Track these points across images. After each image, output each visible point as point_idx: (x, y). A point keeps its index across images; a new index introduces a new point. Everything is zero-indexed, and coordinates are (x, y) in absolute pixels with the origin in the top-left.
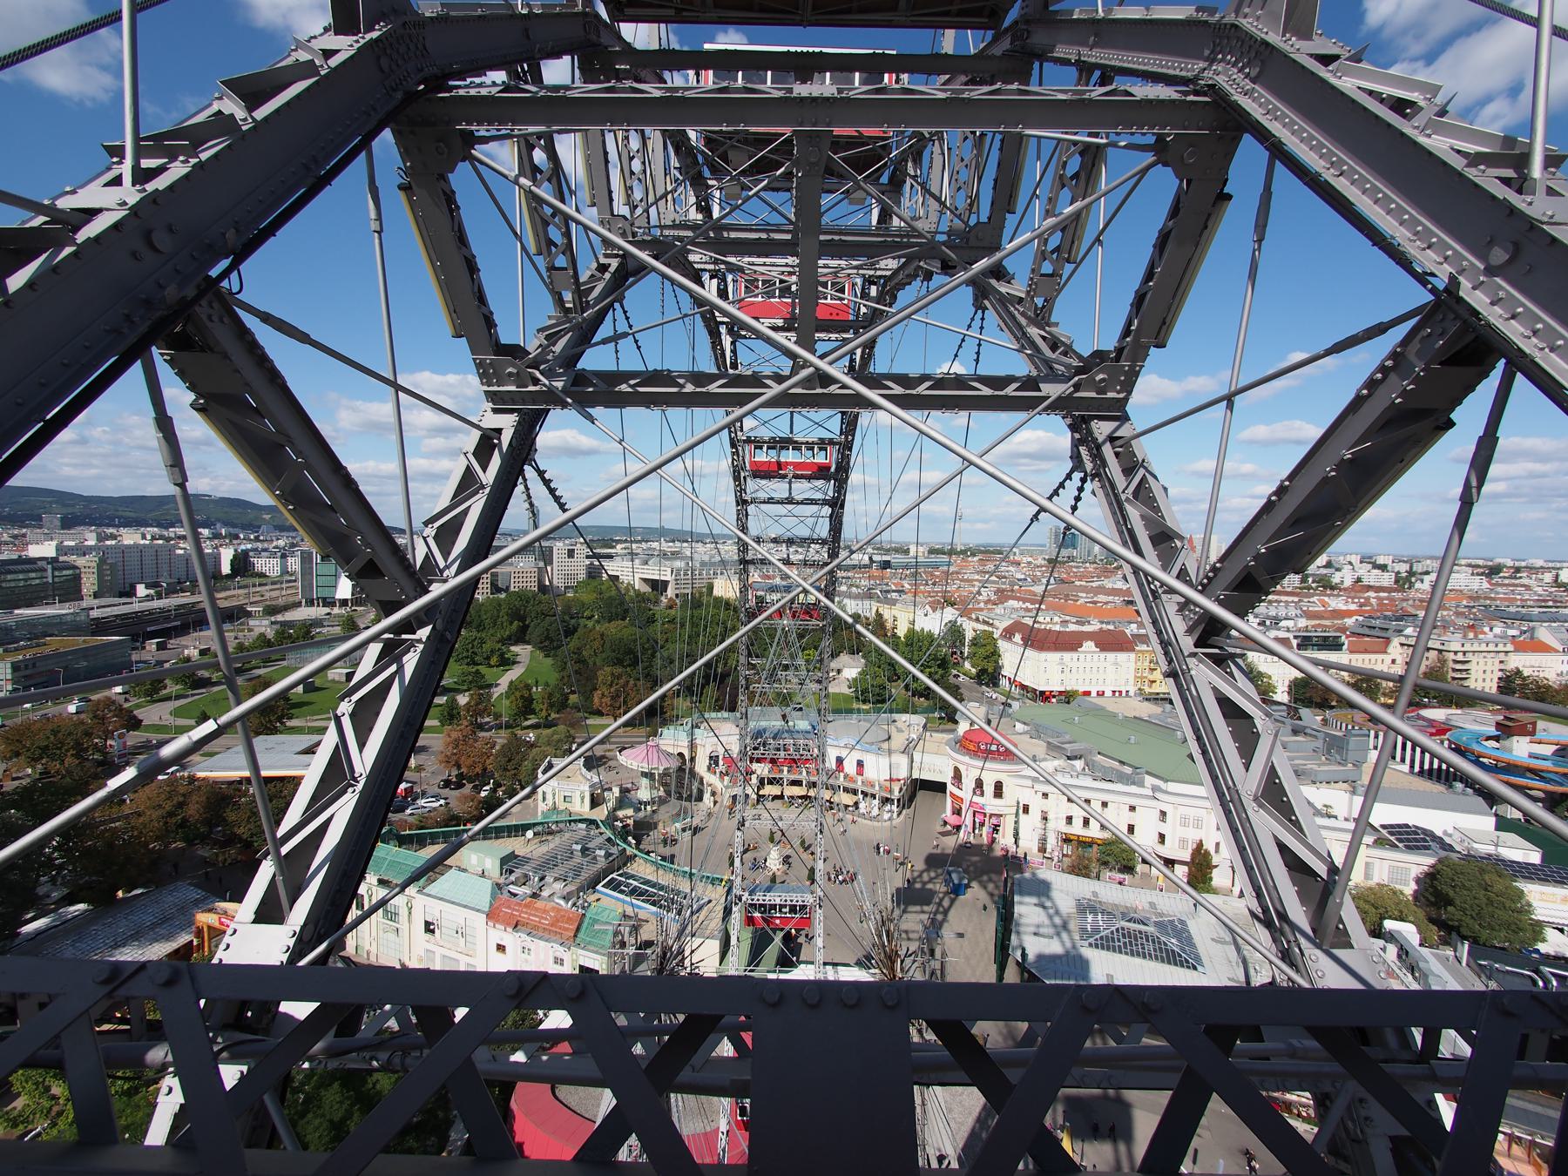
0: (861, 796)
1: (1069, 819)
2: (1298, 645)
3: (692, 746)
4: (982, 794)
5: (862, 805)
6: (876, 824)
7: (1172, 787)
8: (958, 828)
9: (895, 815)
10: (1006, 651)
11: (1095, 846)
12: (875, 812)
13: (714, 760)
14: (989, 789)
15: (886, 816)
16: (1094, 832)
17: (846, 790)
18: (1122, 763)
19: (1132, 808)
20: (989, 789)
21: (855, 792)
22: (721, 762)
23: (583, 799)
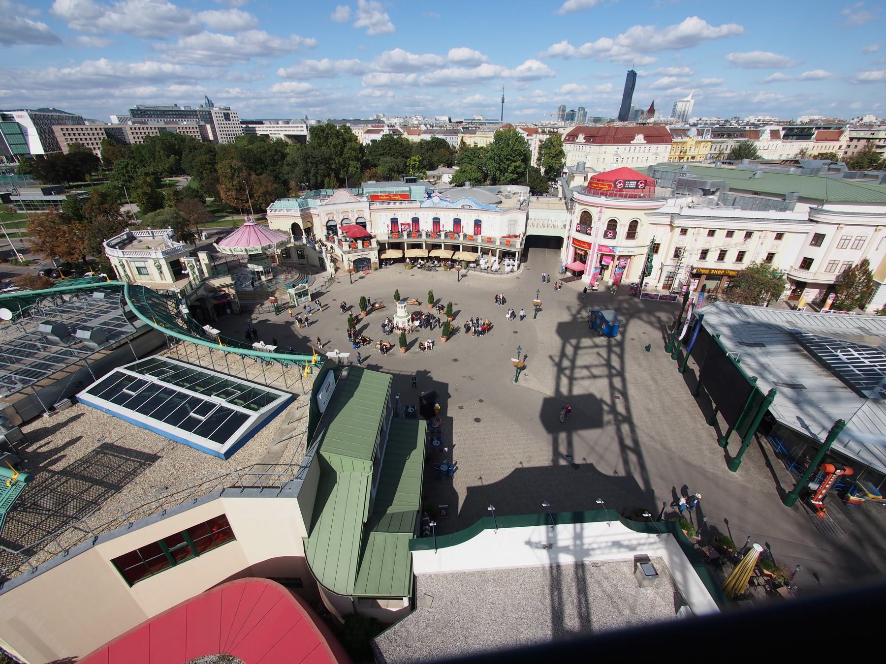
0: (480, 253)
1: (704, 254)
2: (784, 136)
3: (306, 215)
4: (614, 237)
5: (482, 262)
6: (497, 276)
7: (826, 207)
8: (579, 274)
9: (515, 268)
10: (569, 151)
11: (725, 278)
12: (496, 266)
13: (331, 229)
14: (622, 230)
15: (508, 269)
16: (730, 264)
17: (466, 249)
18: (755, 193)
19: (779, 236)
20: (622, 230)
21: (474, 250)
22: (340, 232)
23: (159, 268)
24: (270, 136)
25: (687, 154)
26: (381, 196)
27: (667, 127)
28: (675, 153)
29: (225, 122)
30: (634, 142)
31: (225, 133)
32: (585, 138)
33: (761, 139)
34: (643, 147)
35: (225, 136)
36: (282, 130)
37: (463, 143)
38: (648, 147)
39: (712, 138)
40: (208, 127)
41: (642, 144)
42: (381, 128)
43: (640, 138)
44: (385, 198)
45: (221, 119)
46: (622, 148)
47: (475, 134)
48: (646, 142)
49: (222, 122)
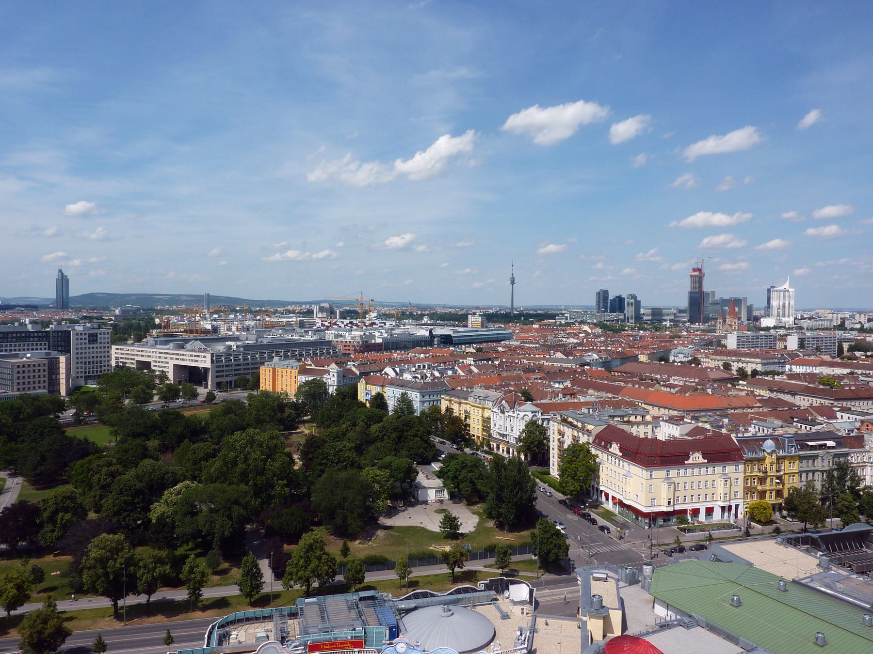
25: (769, 474)
26: (323, 645)
27: (733, 436)
28: (751, 473)
29: (88, 346)
30: (690, 461)
31: (83, 360)
32: (621, 449)
33: (867, 448)
34: (703, 470)
35: (83, 365)
36: (172, 358)
37: (449, 410)
38: (710, 469)
39: (799, 450)
40: (62, 359)
41: (699, 465)
42: (326, 368)
43: (697, 457)
44: (328, 647)
46: (673, 473)
47: (467, 399)
48: (706, 461)
49: (84, 346)
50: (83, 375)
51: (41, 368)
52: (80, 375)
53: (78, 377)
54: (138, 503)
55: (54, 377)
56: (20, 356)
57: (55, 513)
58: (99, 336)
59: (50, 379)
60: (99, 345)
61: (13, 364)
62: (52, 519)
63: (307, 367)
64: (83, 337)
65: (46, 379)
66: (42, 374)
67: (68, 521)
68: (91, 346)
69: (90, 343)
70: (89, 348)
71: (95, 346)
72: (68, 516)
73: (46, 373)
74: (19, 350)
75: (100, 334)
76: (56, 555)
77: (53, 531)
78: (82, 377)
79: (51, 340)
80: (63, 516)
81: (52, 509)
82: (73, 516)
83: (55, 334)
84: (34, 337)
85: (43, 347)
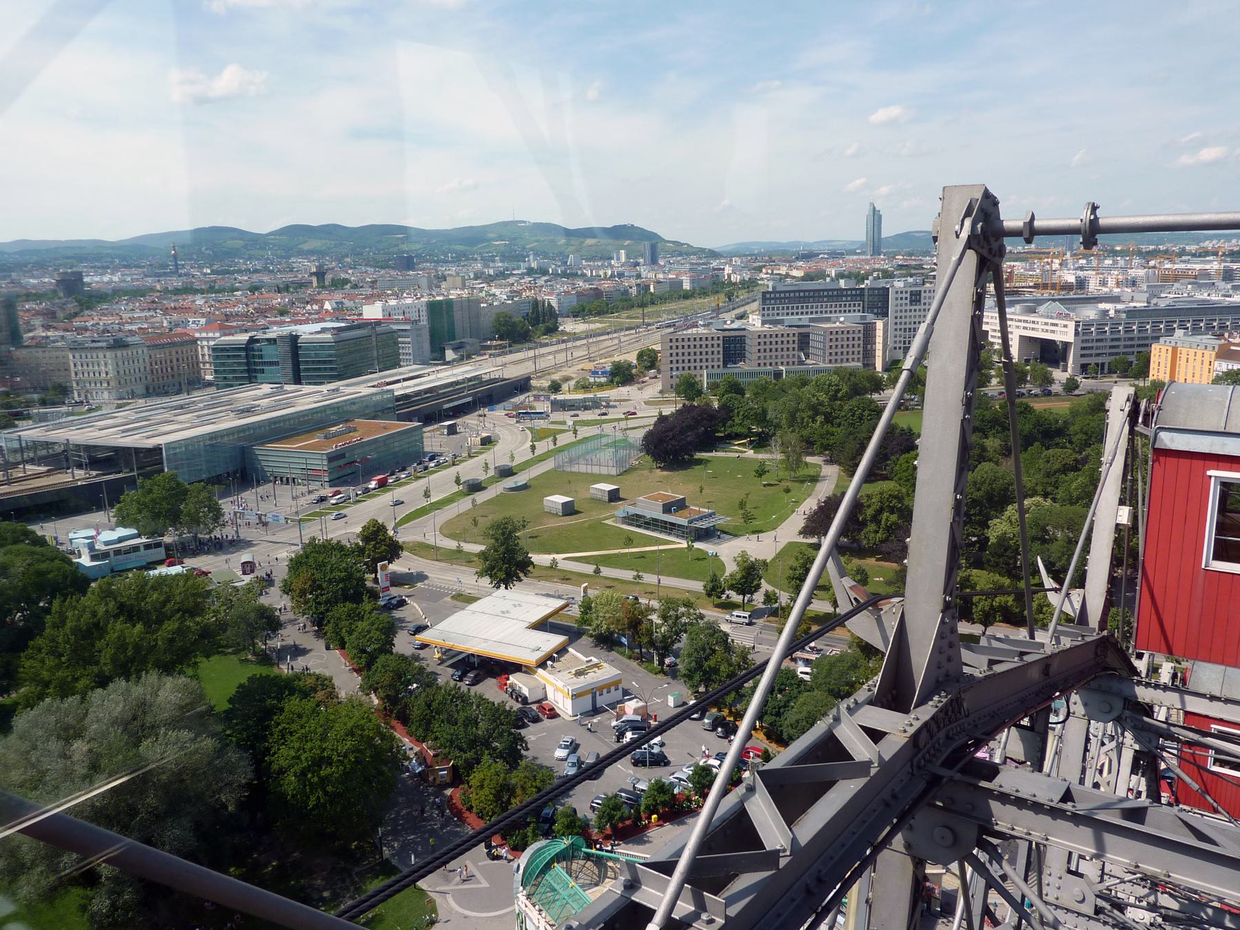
24: (990, 333)
29: (908, 308)
31: (903, 327)
35: (902, 333)
36: (1018, 327)
40: (880, 325)
45: (904, 301)
49: (904, 308)
50: (902, 345)
51: (856, 336)
52: (898, 345)
53: (895, 348)
54: (974, 515)
55: (869, 346)
56: (833, 319)
57: (880, 511)
58: (923, 294)
59: (865, 350)
60: (922, 307)
61: (825, 330)
62: (876, 518)
63: (1232, 348)
64: (904, 295)
65: (861, 349)
66: (856, 343)
67: (894, 523)
68: (913, 308)
69: (911, 305)
70: (911, 311)
71: (917, 307)
72: (894, 518)
73: (861, 342)
74: (831, 312)
75: (925, 292)
76: (878, 560)
77: (877, 532)
78: (900, 348)
79: (866, 299)
80: (888, 517)
81: (876, 506)
82: (899, 517)
83: (871, 292)
84: (847, 296)
85: (856, 308)
